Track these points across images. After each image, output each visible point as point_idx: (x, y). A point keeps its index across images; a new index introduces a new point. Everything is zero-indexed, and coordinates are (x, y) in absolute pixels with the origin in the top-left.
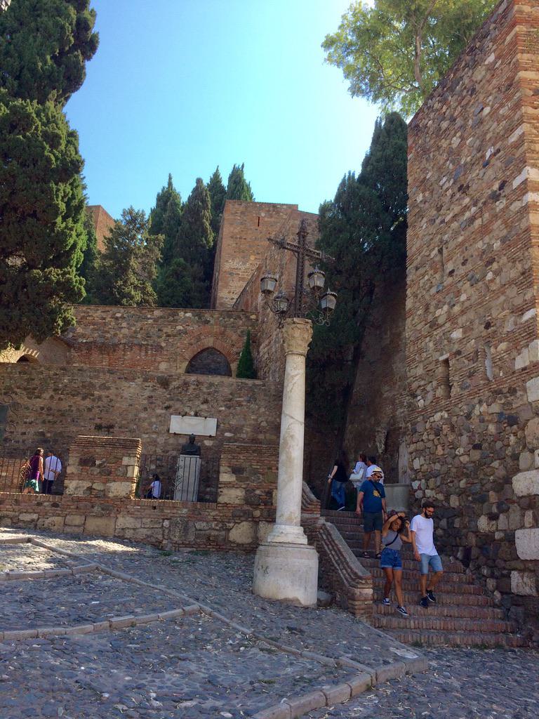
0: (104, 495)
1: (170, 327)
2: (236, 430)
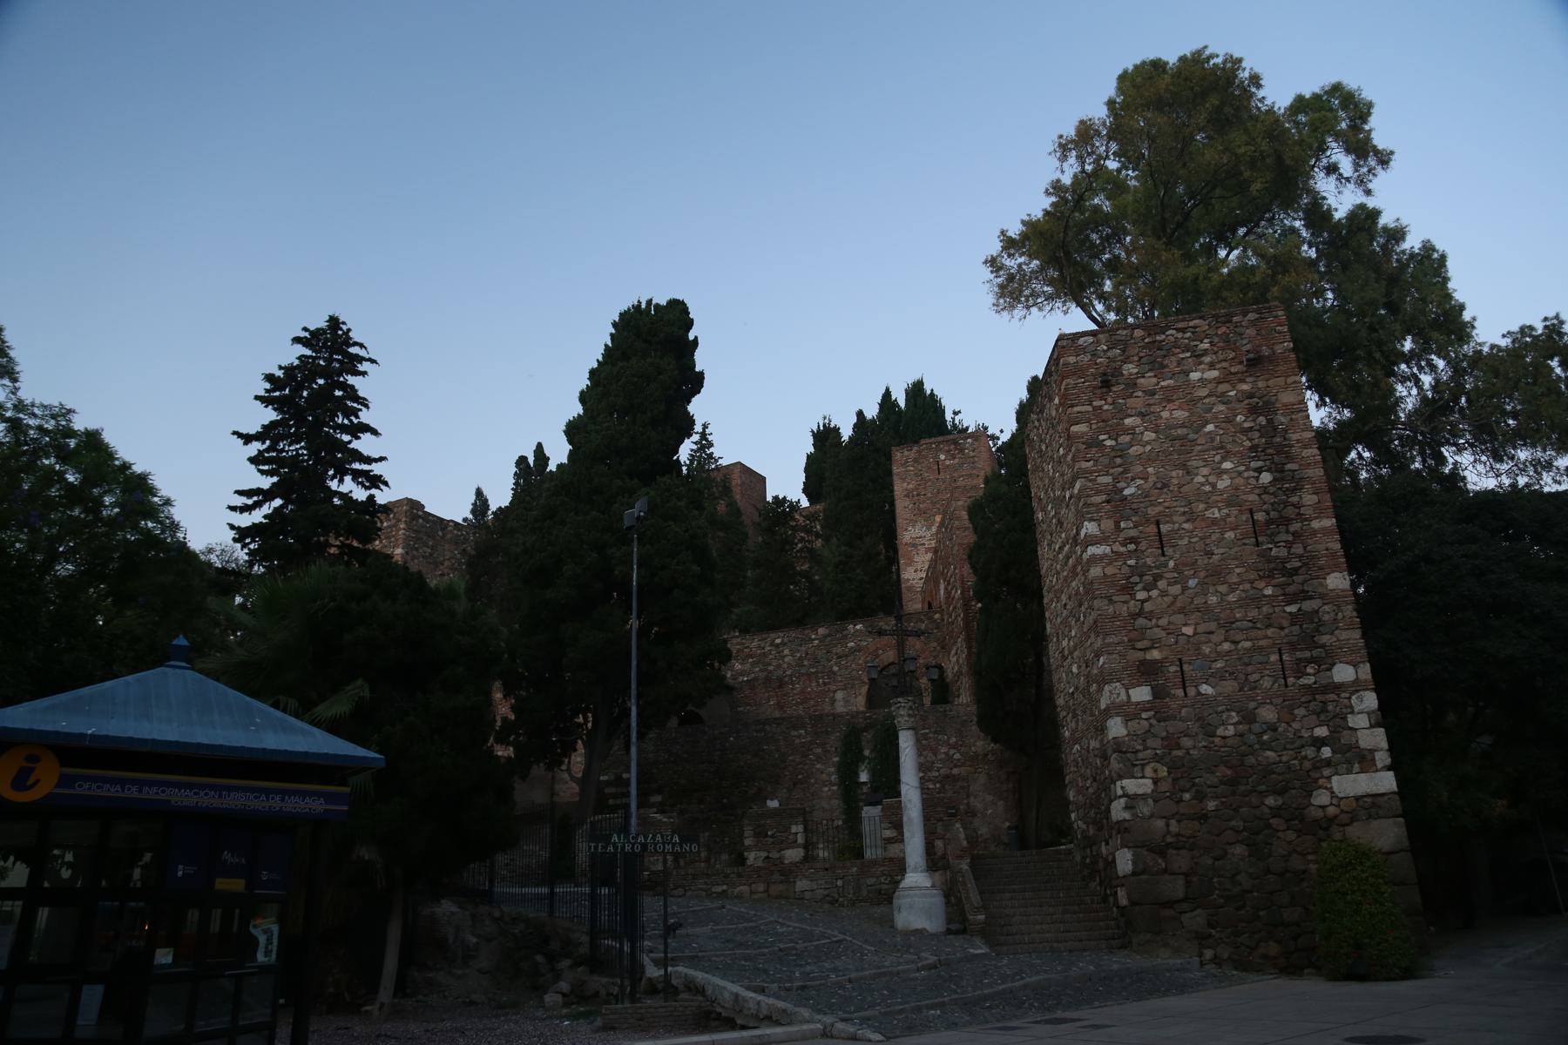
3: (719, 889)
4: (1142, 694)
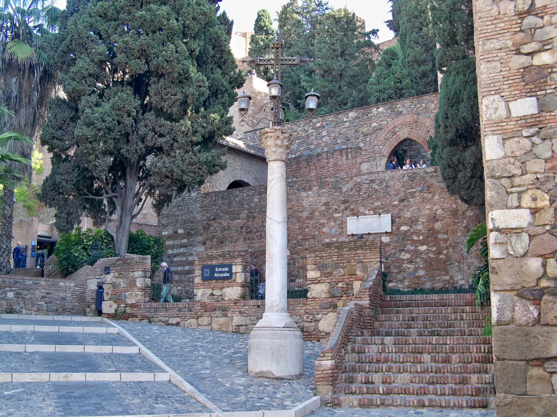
0: (222, 299)
1: (365, 126)
2: (412, 221)
3: (174, 321)
4: (526, 106)
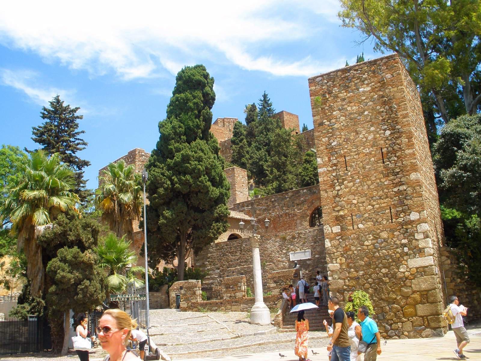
1: (297, 200)
4: (337, 229)
